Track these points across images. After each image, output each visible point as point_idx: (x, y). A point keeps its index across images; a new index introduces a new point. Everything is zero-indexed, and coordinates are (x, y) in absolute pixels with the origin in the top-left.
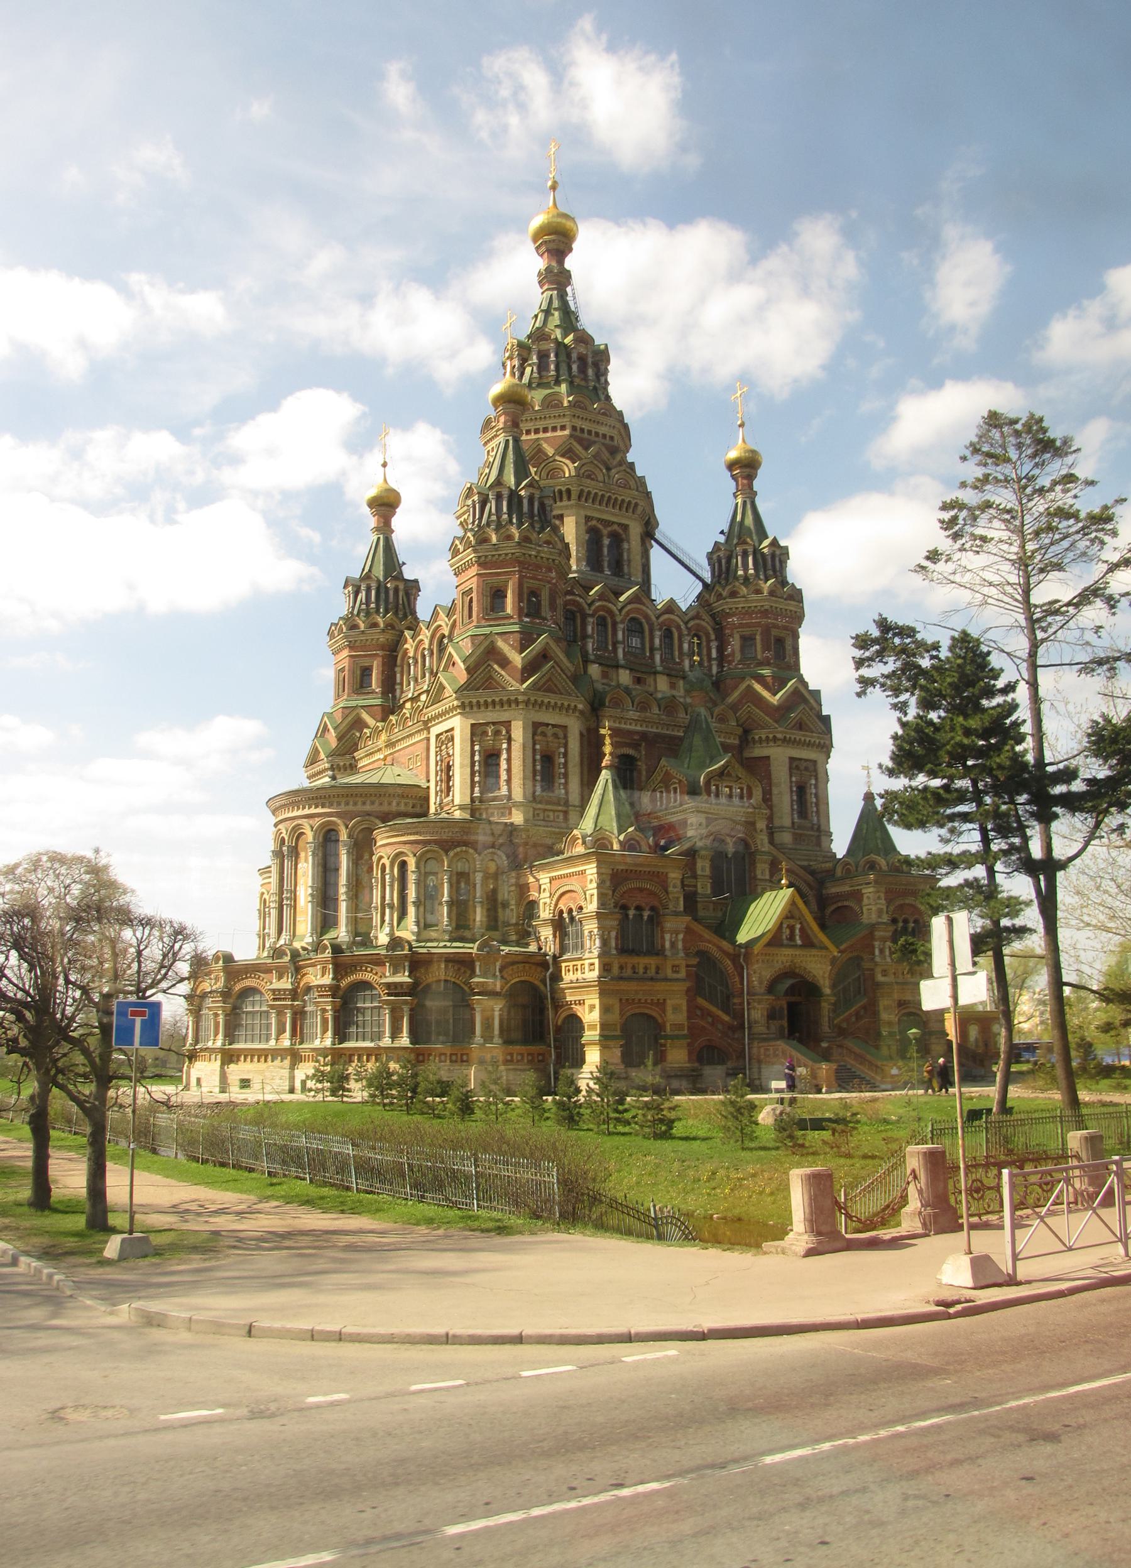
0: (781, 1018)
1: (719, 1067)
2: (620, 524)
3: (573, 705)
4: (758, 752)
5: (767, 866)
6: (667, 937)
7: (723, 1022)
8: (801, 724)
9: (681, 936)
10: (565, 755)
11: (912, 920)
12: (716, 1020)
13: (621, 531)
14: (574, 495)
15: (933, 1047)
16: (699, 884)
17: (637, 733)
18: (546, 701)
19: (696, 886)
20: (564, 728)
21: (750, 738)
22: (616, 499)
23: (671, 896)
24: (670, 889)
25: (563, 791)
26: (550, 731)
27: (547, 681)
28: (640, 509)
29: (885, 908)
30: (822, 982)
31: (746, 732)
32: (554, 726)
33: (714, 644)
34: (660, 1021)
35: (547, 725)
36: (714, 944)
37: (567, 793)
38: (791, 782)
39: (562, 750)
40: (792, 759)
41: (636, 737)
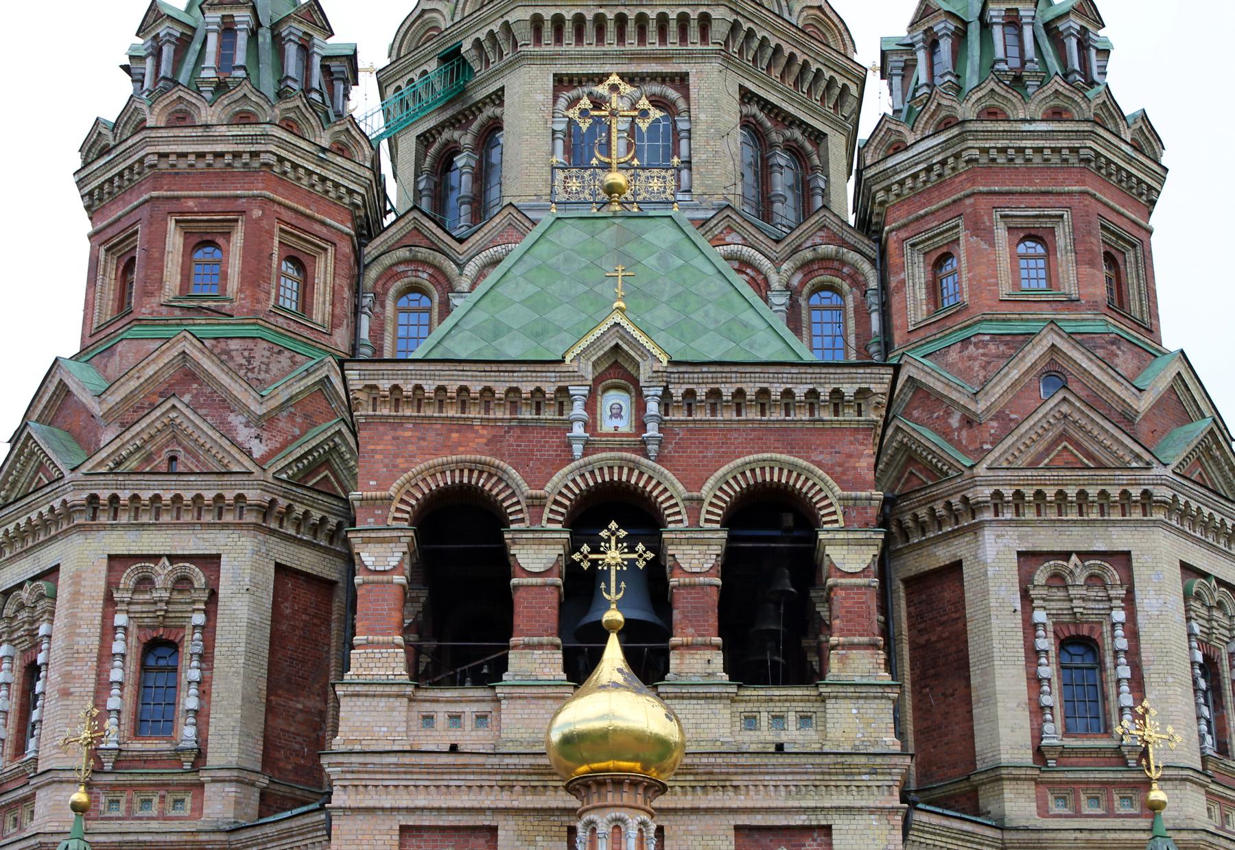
2: (663, 78)
10: (208, 631)
13: (672, 94)
14: (524, 34)
18: (146, 495)
20: (211, 562)
22: (642, 18)
25: (189, 732)
26: (163, 574)
28: (719, 31)
32: (172, 558)
33: (873, 300)
35: (156, 558)
38: (1030, 628)
39: (199, 619)
40: (1028, 558)
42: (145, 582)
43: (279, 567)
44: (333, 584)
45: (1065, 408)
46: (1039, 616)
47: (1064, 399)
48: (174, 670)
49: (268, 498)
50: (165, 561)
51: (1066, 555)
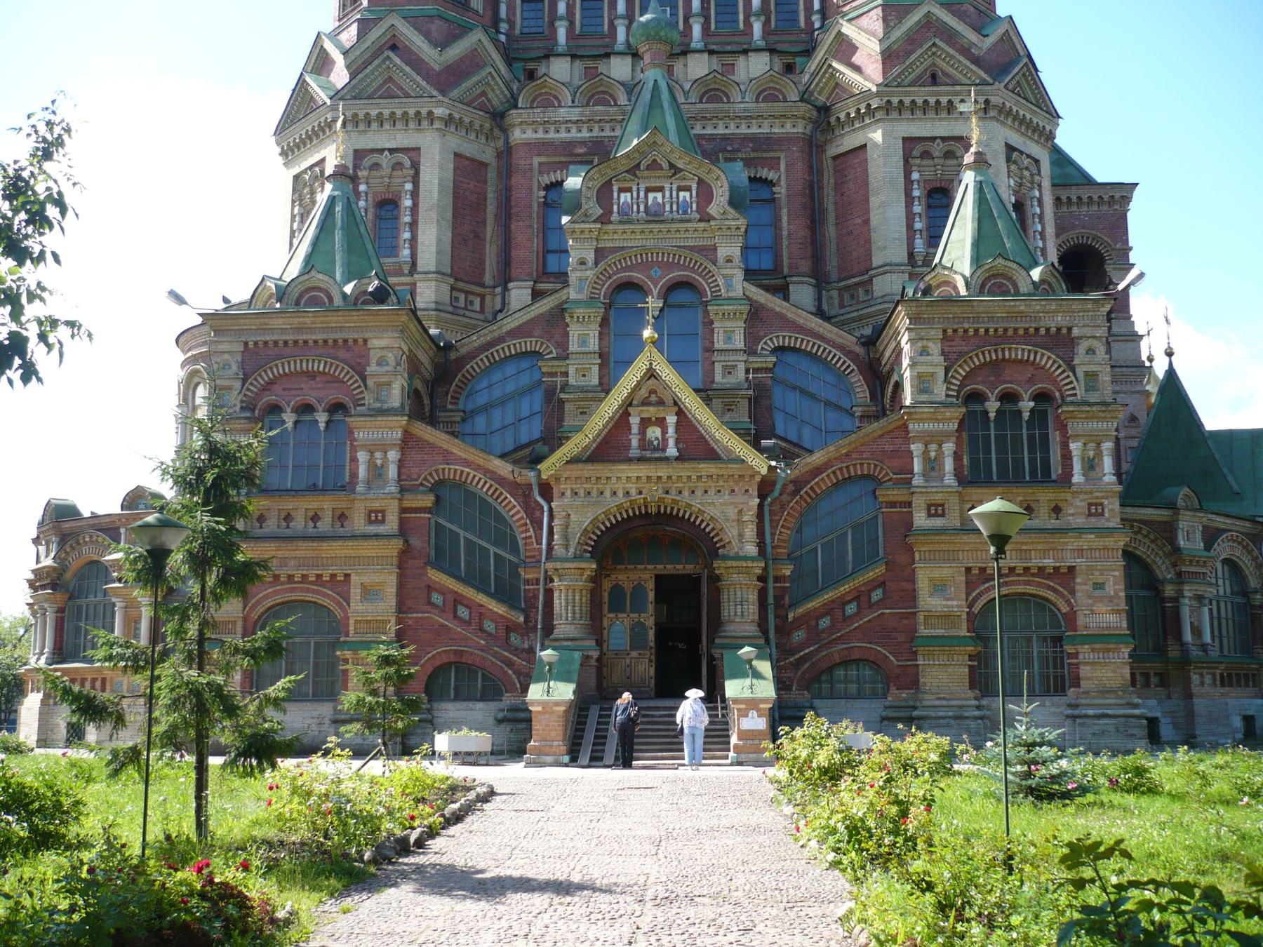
0: (638, 607)
1: (480, 705)
3: (424, 111)
4: (849, 141)
5: (738, 327)
6: (362, 456)
7: (496, 618)
8: (934, 76)
9: (393, 455)
10: (415, 194)
11: (1026, 396)
12: (481, 613)
15: (1084, 671)
16: (572, 370)
17: (583, 143)
18: (374, 113)
19: (566, 374)
20: (413, 152)
21: (833, 120)
23: (370, 382)
24: (372, 368)
25: (406, 252)
27: (385, 82)
29: (941, 372)
30: (731, 533)
31: (825, 110)
32: (392, 151)
34: (339, 613)
35: (381, 151)
36: (478, 468)
37: (414, 256)
38: (908, 182)
39: (409, 186)
41: (580, 151)
42: (375, 166)
43: (456, 155)
44: (485, 165)
45: (934, 49)
46: (915, 176)
47: (934, 44)
48: (397, 218)
49: (448, 112)
50: (386, 152)
51: (933, 139)
